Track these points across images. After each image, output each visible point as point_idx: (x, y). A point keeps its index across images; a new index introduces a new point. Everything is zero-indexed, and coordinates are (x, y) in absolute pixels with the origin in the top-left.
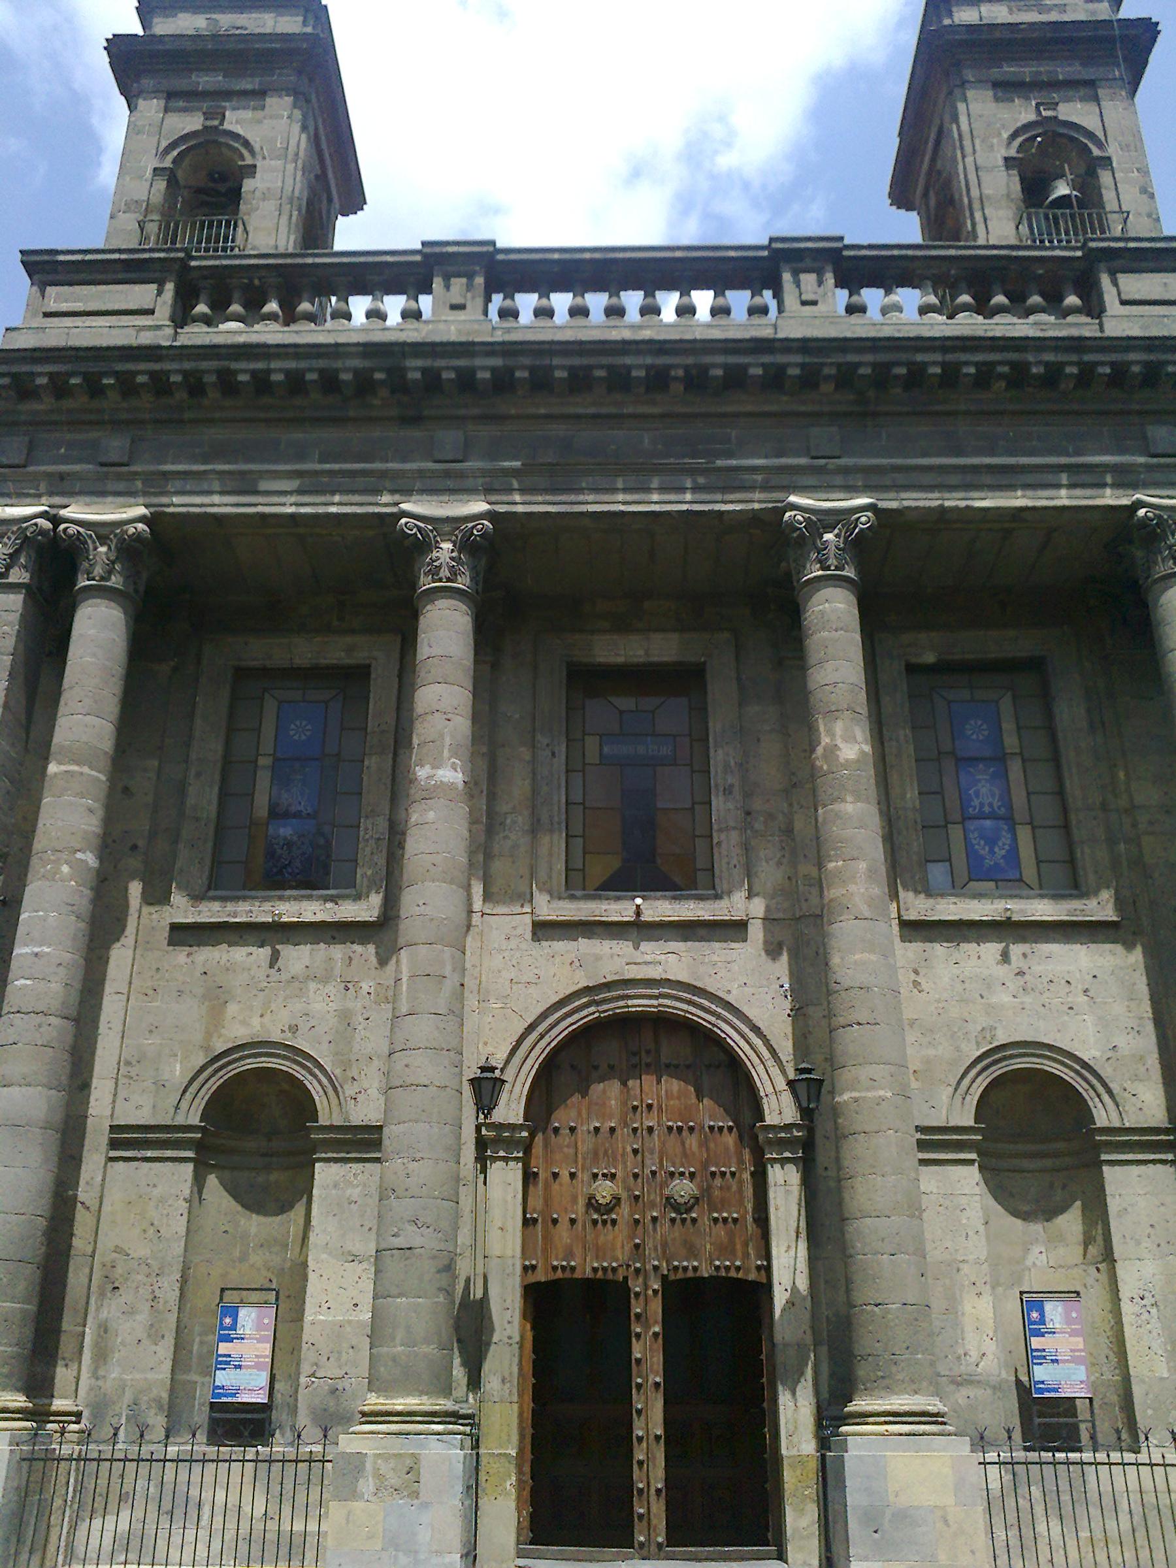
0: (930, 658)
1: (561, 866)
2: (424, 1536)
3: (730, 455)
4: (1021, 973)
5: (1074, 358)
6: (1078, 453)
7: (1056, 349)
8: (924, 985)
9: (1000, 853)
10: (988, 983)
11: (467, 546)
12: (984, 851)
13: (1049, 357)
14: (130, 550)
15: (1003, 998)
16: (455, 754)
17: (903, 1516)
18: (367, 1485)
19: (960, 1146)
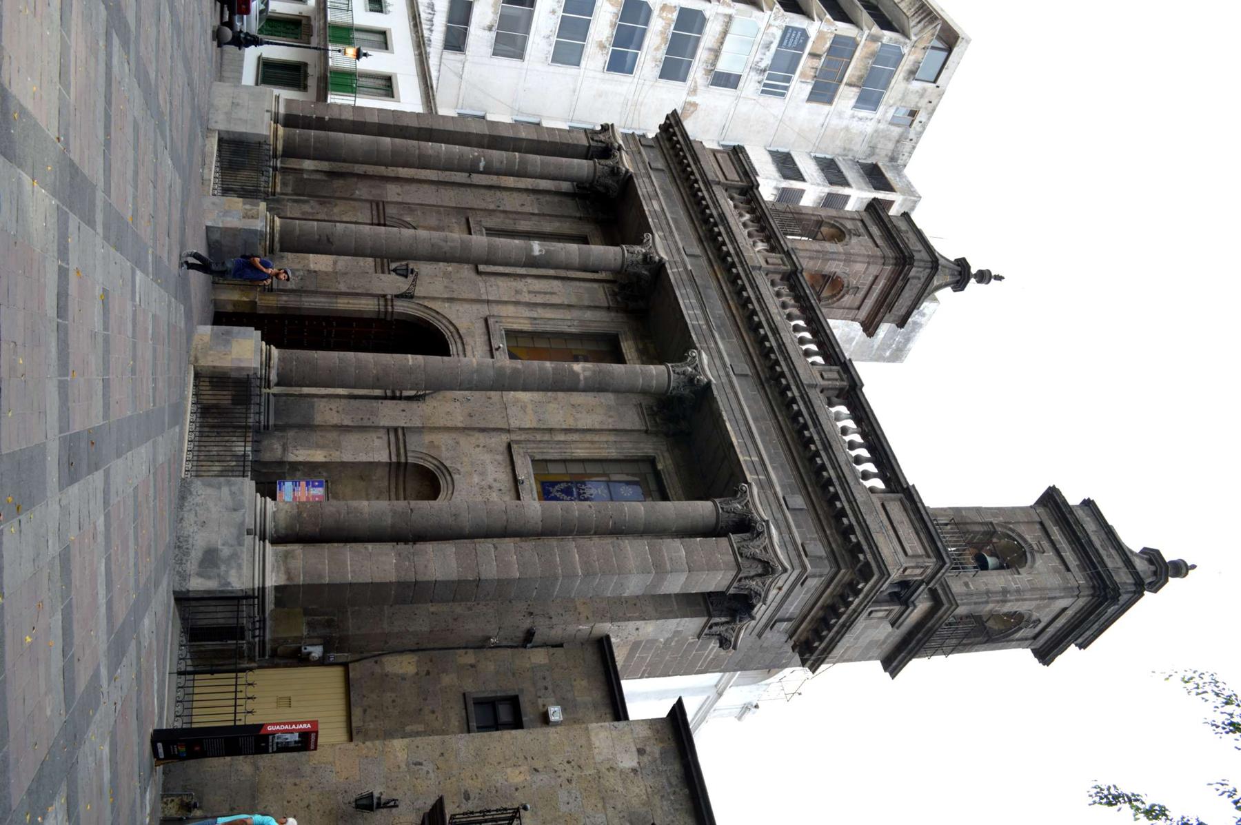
0: (660, 467)
1: (516, 327)
2: (229, 219)
3: (722, 338)
4: (490, 487)
5: (820, 447)
6: (774, 468)
7: (821, 439)
8: (477, 450)
9: (558, 495)
10: (483, 474)
11: (647, 259)
12: (556, 488)
13: (816, 437)
14: (615, 171)
15: (476, 479)
16: (547, 251)
17: (228, 342)
18: (248, 207)
19: (398, 455)
